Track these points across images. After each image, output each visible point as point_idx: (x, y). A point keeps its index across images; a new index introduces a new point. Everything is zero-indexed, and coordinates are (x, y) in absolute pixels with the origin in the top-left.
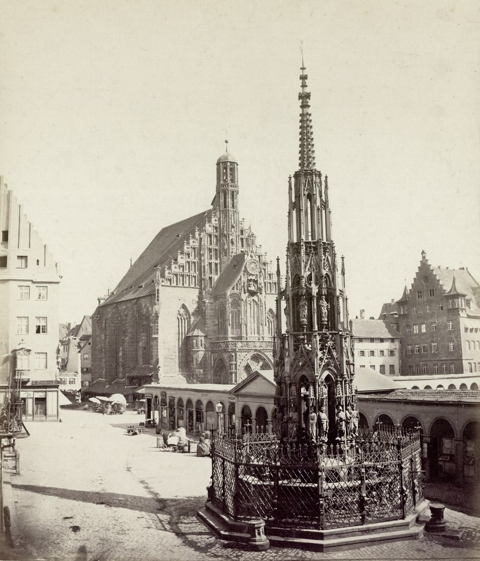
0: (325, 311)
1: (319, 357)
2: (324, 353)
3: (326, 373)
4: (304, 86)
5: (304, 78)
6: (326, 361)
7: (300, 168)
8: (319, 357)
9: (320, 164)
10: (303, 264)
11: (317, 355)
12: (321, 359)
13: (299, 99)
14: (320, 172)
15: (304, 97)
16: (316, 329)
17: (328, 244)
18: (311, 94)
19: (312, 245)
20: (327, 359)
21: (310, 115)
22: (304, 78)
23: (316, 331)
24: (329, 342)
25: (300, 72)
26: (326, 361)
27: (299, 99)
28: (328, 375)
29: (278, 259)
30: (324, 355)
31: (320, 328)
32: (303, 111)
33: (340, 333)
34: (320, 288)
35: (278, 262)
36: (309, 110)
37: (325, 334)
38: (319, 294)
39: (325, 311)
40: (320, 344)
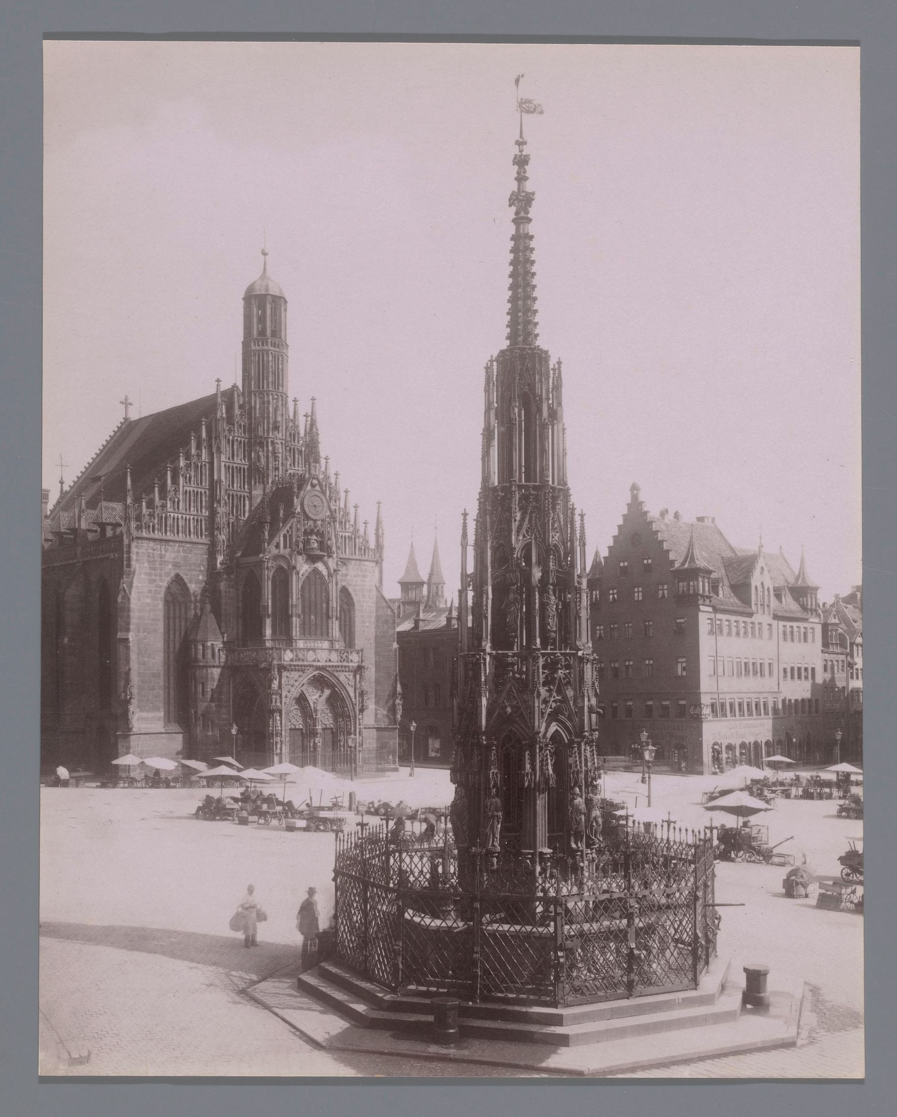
0: (552, 610)
1: (542, 698)
2: (550, 691)
3: (554, 727)
4: (521, 178)
5: (521, 162)
6: (554, 705)
7: (508, 342)
8: (542, 698)
9: (546, 338)
10: (515, 526)
11: (539, 695)
12: (545, 702)
13: (510, 206)
14: (547, 352)
15: (522, 201)
16: (539, 646)
17: (560, 490)
18: (536, 196)
19: (532, 492)
20: (555, 701)
21: (531, 237)
22: (521, 162)
23: (538, 650)
24: (560, 671)
25: (516, 150)
26: (554, 705)
27: (510, 206)
28: (557, 730)
29: (465, 515)
30: (550, 696)
31: (544, 645)
32: (518, 229)
33: (580, 653)
34: (546, 572)
35: (465, 519)
36: (531, 229)
37: (554, 654)
38: (544, 581)
39: (552, 610)
40: (543, 673)
